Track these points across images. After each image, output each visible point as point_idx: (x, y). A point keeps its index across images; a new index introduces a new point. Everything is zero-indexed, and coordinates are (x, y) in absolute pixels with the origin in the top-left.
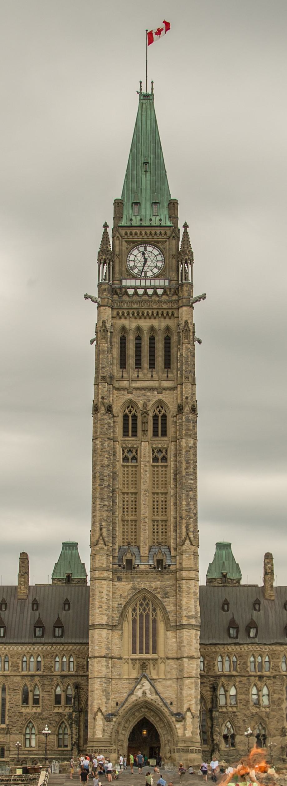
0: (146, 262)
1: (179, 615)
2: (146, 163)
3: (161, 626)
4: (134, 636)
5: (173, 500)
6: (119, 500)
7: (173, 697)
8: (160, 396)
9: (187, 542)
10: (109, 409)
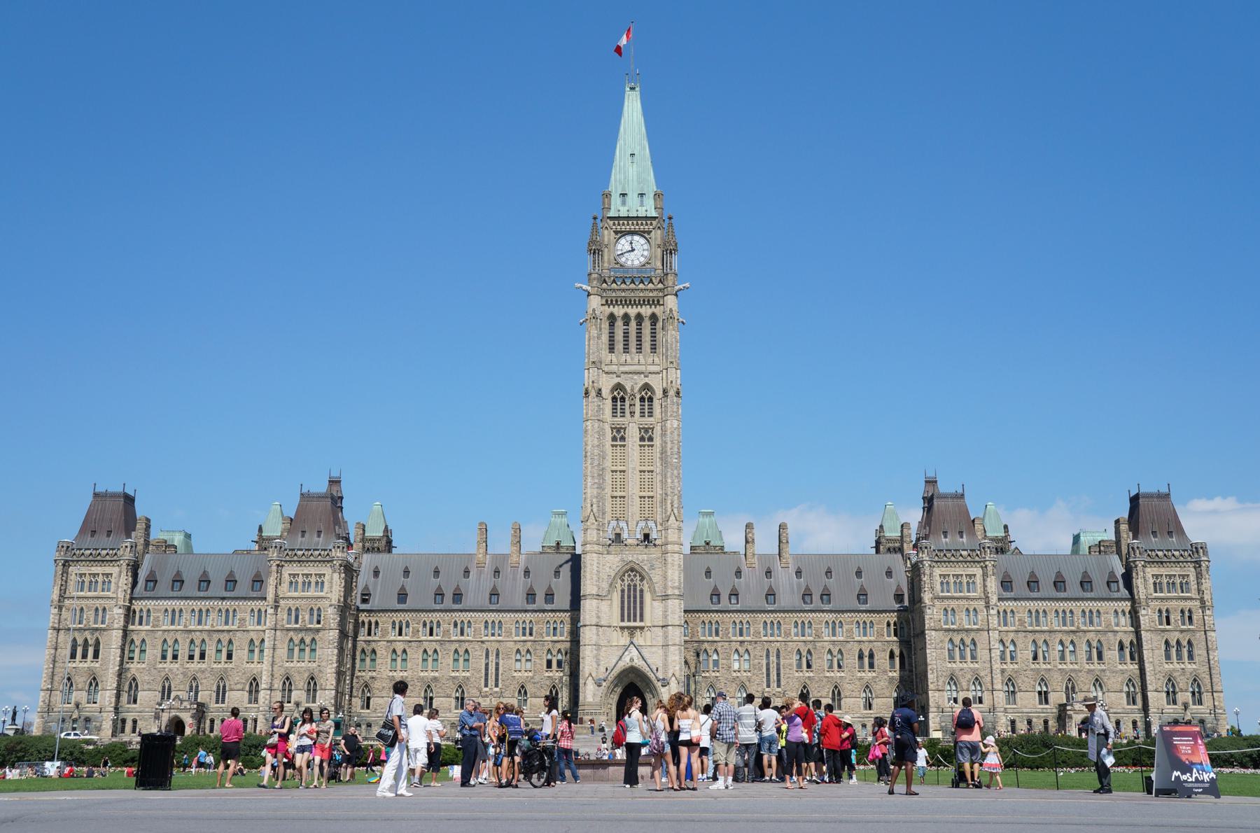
1: (665, 587)
2: (632, 155)
3: (647, 597)
4: (623, 602)
5: (659, 478)
6: (608, 476)
7: (660, 665)
8: (646, 380)
9: (672, 518)
10: (599, 393)
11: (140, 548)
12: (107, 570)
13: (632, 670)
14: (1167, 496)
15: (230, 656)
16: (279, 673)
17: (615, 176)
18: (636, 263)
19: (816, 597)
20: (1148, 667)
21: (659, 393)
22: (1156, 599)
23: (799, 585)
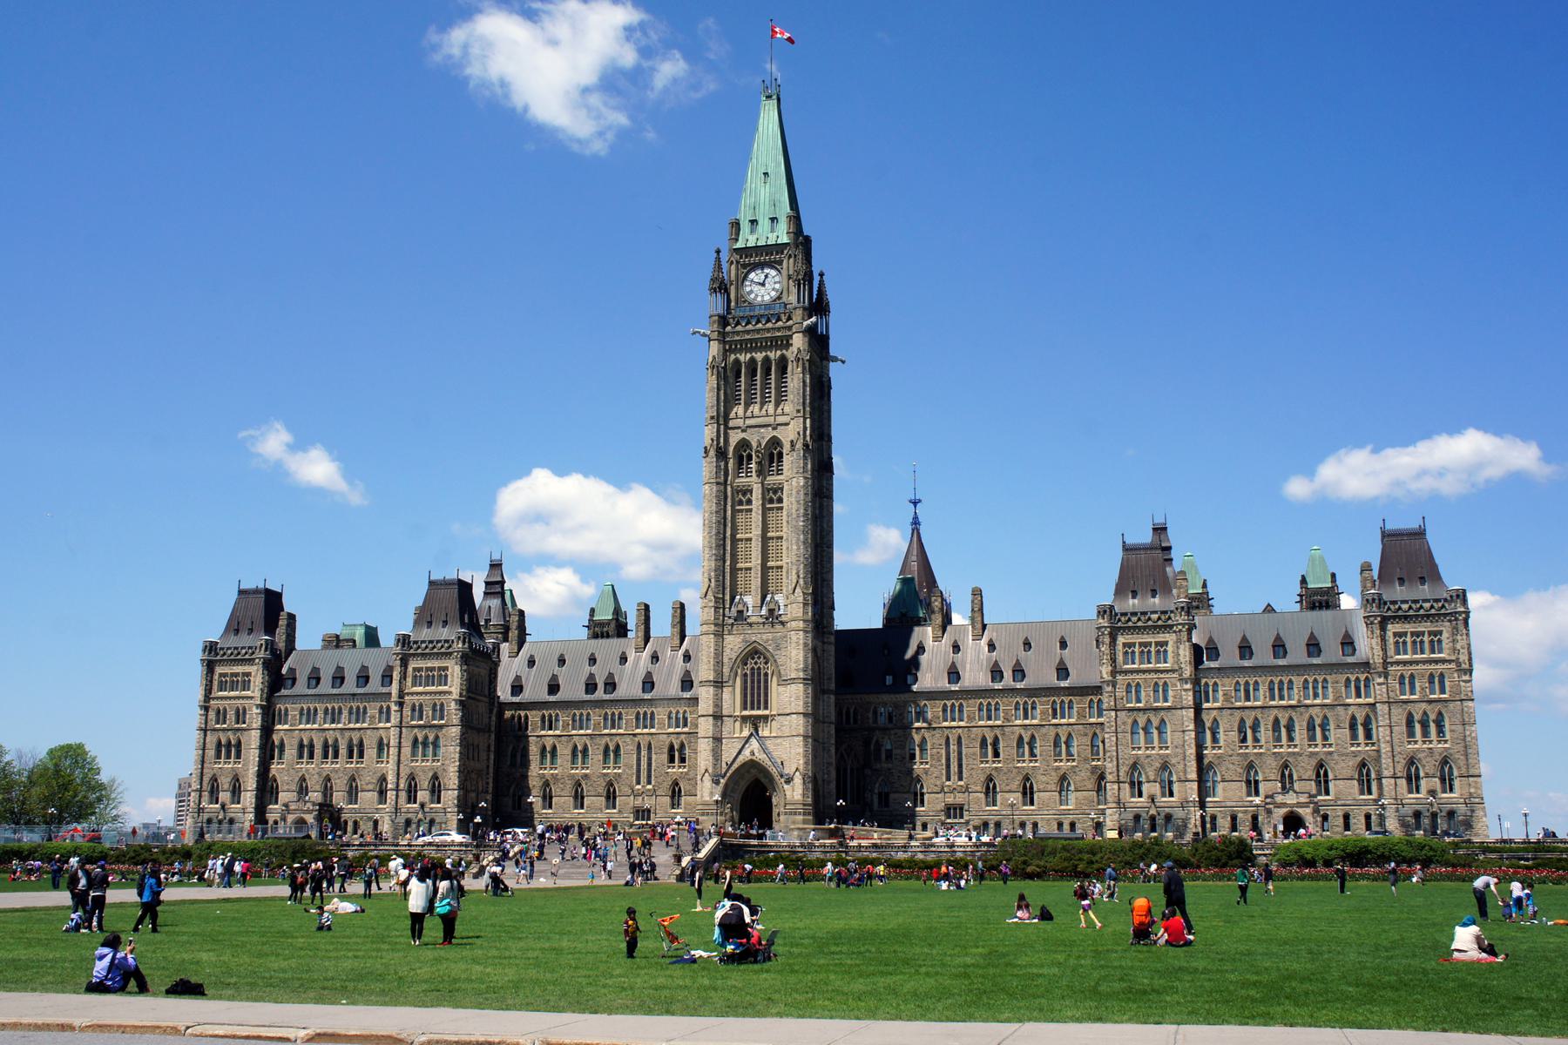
0: (764, 287)
7: (784, 757)
8: (775, 433)
11: (281, 643)
12: (247, 669)
13: (752, 765)
14: (1420, 534)
15: (361, 755)
16: (404, 773)
17: (746, 200)
18: (767, 298)
19: (1008, 674)
20: (1385, 748)
21: (786, 448)
22: (1398, 663)
23: (989, 659)
